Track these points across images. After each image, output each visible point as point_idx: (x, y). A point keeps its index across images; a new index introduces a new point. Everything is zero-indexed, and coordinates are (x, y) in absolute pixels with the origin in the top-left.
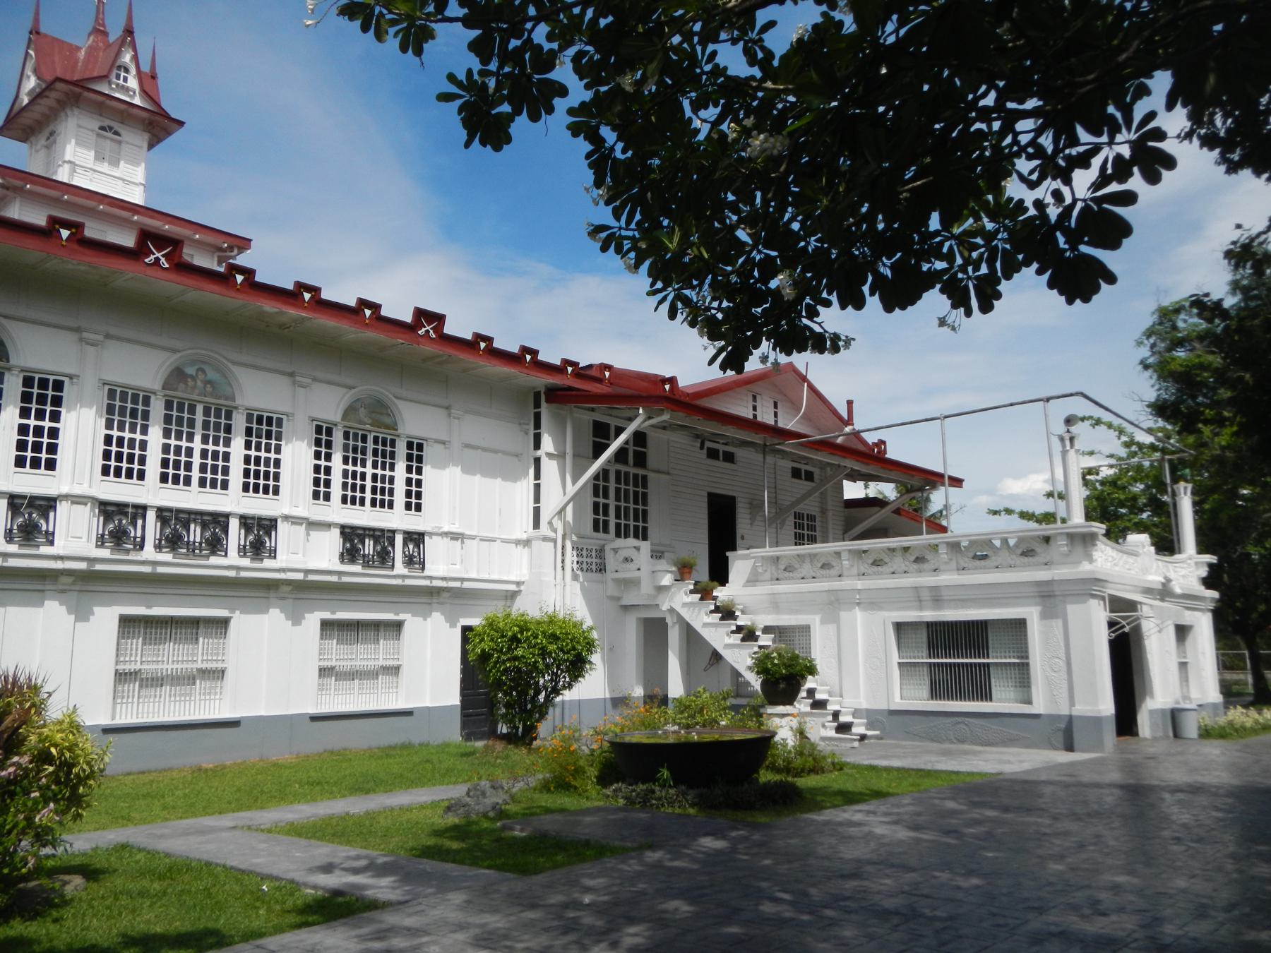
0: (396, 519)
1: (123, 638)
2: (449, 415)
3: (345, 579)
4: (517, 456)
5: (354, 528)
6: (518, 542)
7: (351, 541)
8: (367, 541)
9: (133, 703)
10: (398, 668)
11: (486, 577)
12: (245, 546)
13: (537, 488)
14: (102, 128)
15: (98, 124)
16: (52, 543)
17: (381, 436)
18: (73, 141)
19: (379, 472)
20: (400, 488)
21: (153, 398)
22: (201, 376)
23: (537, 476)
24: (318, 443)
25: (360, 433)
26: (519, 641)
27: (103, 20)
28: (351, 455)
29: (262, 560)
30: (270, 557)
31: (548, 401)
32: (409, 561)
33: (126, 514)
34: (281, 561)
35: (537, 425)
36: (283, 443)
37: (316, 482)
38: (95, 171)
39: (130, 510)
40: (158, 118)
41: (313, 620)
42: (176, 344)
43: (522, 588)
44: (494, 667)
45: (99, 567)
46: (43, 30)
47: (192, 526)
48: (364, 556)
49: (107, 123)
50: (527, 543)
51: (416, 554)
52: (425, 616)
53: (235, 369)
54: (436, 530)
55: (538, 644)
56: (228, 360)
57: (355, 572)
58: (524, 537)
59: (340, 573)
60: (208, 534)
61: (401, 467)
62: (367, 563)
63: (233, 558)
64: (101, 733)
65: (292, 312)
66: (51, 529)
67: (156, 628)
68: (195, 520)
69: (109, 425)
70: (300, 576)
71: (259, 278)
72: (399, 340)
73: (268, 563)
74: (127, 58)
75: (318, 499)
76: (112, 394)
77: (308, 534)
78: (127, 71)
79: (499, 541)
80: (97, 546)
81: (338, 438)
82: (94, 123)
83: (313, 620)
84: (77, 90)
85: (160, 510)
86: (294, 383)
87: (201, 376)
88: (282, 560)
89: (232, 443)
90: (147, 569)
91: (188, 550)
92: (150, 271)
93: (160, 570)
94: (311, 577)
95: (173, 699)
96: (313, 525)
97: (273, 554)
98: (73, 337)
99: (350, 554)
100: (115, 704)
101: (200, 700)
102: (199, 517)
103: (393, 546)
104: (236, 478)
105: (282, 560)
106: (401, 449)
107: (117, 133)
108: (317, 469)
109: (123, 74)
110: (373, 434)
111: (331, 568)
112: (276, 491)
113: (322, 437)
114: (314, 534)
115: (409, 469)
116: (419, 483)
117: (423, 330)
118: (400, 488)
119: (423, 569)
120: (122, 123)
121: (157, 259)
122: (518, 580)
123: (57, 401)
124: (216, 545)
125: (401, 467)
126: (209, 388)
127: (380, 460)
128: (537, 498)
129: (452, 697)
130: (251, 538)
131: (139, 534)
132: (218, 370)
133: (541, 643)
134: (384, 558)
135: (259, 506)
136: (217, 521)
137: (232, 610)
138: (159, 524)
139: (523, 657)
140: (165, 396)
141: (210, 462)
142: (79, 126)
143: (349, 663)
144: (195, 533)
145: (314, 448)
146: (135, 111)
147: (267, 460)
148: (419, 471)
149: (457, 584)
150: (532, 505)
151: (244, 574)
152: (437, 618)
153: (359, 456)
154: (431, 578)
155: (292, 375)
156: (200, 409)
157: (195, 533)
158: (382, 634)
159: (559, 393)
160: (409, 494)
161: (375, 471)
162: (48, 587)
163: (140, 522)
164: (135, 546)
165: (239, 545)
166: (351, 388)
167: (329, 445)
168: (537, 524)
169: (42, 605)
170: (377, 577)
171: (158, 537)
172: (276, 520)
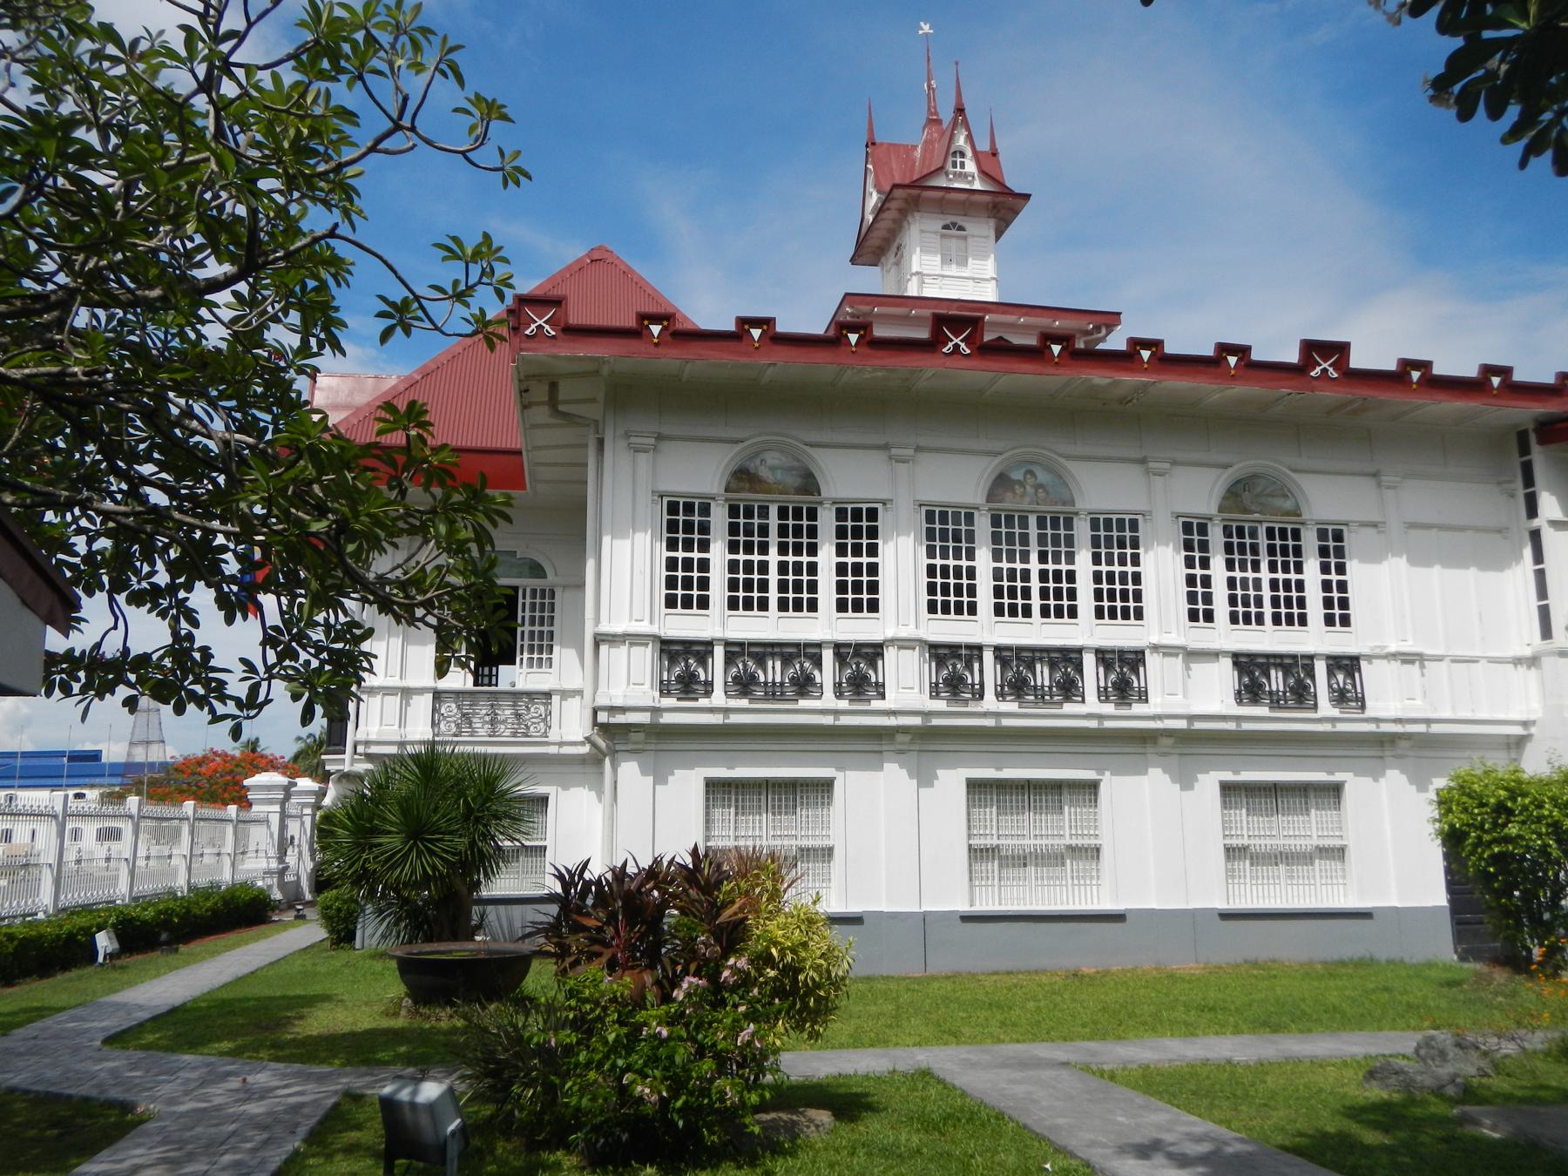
0: (1314, 639)
1: (974, 806)
2: (1379, 485)
3: (1246, 726)
4: (1499, 531)
5: (1252, 656)
6: (1517, 661)
7: (1250, 674)
8: (1273, 672)
9: (993, 885)
10: (1341, 851)
11: (1468, 715)
12: (1106, 688)
13: (1540, 576)
14: (946, 227)
15: (942, 223)
16: (882, 696)
17: (1277, 526)
18: (918, 249)
19: (1280, 576)
21: (976, 514)
22: (1030, 480)
23: (1538, 557)
24: (1188, 546)
25: (1246, 526)
26: (1510, 812)
27: (935, 108)
28: (1236, 557)
29: (1130, 704)
30: (1140, 700)
31: (1542, 441)
32: (1340, 697)
33: (959, 657)
34: (1155, 705)
35: (1529, 480)
36: (1141, 551)
37: (1192, 597)
38: (943, 276)
39: (963, 652)
40: (1000, 199)
41: (1209, 783)
42: (996, 445)
43: (1533, 730)
44: (1472, 853)
45: (936, 722)
46: (878, 140)
47: (1038, 667)
48: (1271, 693)
49: (949, 219)
50: (1533, 661)
51: (1349, 687)
52: (1376, 775)
53: (1073, 466)
54: (1377, 651)
55: (1545, 817)
56: (1060, 455)
58: (1528, 652)
59: (1238, 719)
60: (1058, 676)
62: (1276, 702)
63: (1092, 704)
64: (959, 921)
65: (1129, 379)
66: (881, 680)
67: (1017, 795)
68: (1041, 659)
69: (931, 553)
70: (1181, 724)
72: (1285, 390)
73: (1137, 709)
74: (961, 141)
75: (1237, 623)
76: (930, 517)
77: (1188, 668)
78: (963, 155)
79: (1483, 662)
80: (931, 697)
81: (1216, 537)
82: (935, 223)
83: (1209, 783)
84: (915, 192)
85: (998, 650)
86: (1147, 471)
87: (1030, 480)
88: (1156, 704)
89: (1077, 558)
90: (990, 722)
91: (1036, 696)
92: (950, 362)
93: (1006, 722)
94: (1198, 725)
95: (1076, 882)
96: (1193, 655)
97: (1143, 697)
98: (881, 456)
99: (1251, 691)
100: (972, 887)
101: (1073, 885)
102: (1045, 655)
103: (1313, 678)
105: (1156, 704)
107: (961, 228)
108: (1191, 580)
109: (959, 160)
110: (1265, 525)
111: (1224, 712)
112: (1139, 614)
113: (1193, 538)
114: (1198, 668)
115: (1325, 569)
116: (1342, 586)
117: (1318, 369)
119: (1363, 707)
121: (957, 346)
122: (1524, 717)
123: (873, 532)
124: (1069, 689)
126: (1041, 493)
127: (1279, 559)
128: (1542, 592)
129: (1436, 895)
130: (1113, 677)
131: (977, 681)
132: (1049, 469)
133: (1551, 816)
134: (1301, 695)
136: (1066, 659)
137: (1101, 771)
138: (998, 667)
139: (1520, 837)
140: (990, 509)
141: (1051, 585)
142: (922, 231)
143: (1268, 842)
144: (1043, 675)
145: (1184, 553)
147: (1123, 576)
148: (1341, 569)
149: (1421, 728)
150: (1534, 603)
151: (1108, 724)
152: (1395, 779)
153: (1249, 557)
154: (1377, 720)
155: (1143, 461)
156: (1032, 520)
157: (1043, 675)
158: (1312, 801)
159: (1559, 426)
160: (1328, 603)
161: (1256, 575)
162: (885, 748)
163: (976, 666)
164: (973, 694)
165: (1099, 687)
166: (1226, 466)
167: (1204, 546)
168: (1546, 632)
169: (881, 768)
170: (1293, 721)
171: (999, 682)
172: (1143, 652)
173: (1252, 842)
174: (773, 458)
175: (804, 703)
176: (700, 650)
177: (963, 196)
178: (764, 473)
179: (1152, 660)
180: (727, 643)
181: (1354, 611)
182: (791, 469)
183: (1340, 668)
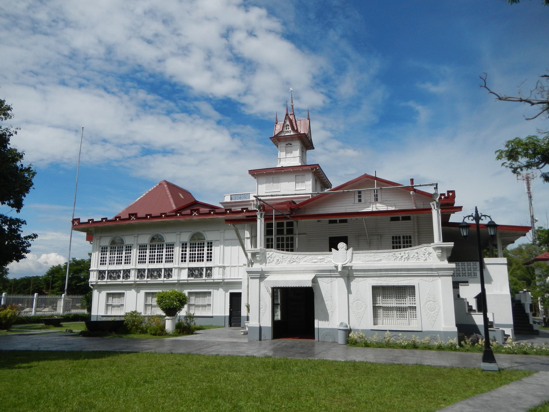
0: (204, 264)
3: (189, 281)
5: (193, 268)
20: (205, 256)
22: (158, 238)
24: (183, 248)
25: (194, 243)
37: (182, 258)
48: (195, 275)
52: (218, 290)
54: (216, 266)
57: (192, 279)
59: (188, 280)
61: (206, 248)
62: (196, 276)
71: (153, 215)
73: (170, 279)
78: (289, 126)
81: (188, 245)
87: (158, 238)
90: (145, 282)
93: (148, 282)
94: (181, 282)
104: (164, 260)
106: (206, 244)
107: (291, 144)
108: (182, 254)
112: (172, 261)
113: (184, 245)
116: (211, 253)
118: (205, 256)
120: (292, 141)
124: (160, 276)
125: (206, 248)
126: (159, 240)
134: (201, 275)
135: (169, 265)
136: (159, 270)
142: (281, 147)
144: (155, 274)
146: (293, 136)
151: (165, 282)
152: (221, 290)
154: (214, 280)
160: (208, 257)
169: (131, 290)
172: (172, 269)
173: (196, 303)
174: (118, 238)
175: (118, 280)
176: (104, 272)
177: (289, 136)
178: (116, 241)
179: (173, 269)
180: (108, 271)
181: (212, 258)
182: (120, 240)
183: (209, 269)
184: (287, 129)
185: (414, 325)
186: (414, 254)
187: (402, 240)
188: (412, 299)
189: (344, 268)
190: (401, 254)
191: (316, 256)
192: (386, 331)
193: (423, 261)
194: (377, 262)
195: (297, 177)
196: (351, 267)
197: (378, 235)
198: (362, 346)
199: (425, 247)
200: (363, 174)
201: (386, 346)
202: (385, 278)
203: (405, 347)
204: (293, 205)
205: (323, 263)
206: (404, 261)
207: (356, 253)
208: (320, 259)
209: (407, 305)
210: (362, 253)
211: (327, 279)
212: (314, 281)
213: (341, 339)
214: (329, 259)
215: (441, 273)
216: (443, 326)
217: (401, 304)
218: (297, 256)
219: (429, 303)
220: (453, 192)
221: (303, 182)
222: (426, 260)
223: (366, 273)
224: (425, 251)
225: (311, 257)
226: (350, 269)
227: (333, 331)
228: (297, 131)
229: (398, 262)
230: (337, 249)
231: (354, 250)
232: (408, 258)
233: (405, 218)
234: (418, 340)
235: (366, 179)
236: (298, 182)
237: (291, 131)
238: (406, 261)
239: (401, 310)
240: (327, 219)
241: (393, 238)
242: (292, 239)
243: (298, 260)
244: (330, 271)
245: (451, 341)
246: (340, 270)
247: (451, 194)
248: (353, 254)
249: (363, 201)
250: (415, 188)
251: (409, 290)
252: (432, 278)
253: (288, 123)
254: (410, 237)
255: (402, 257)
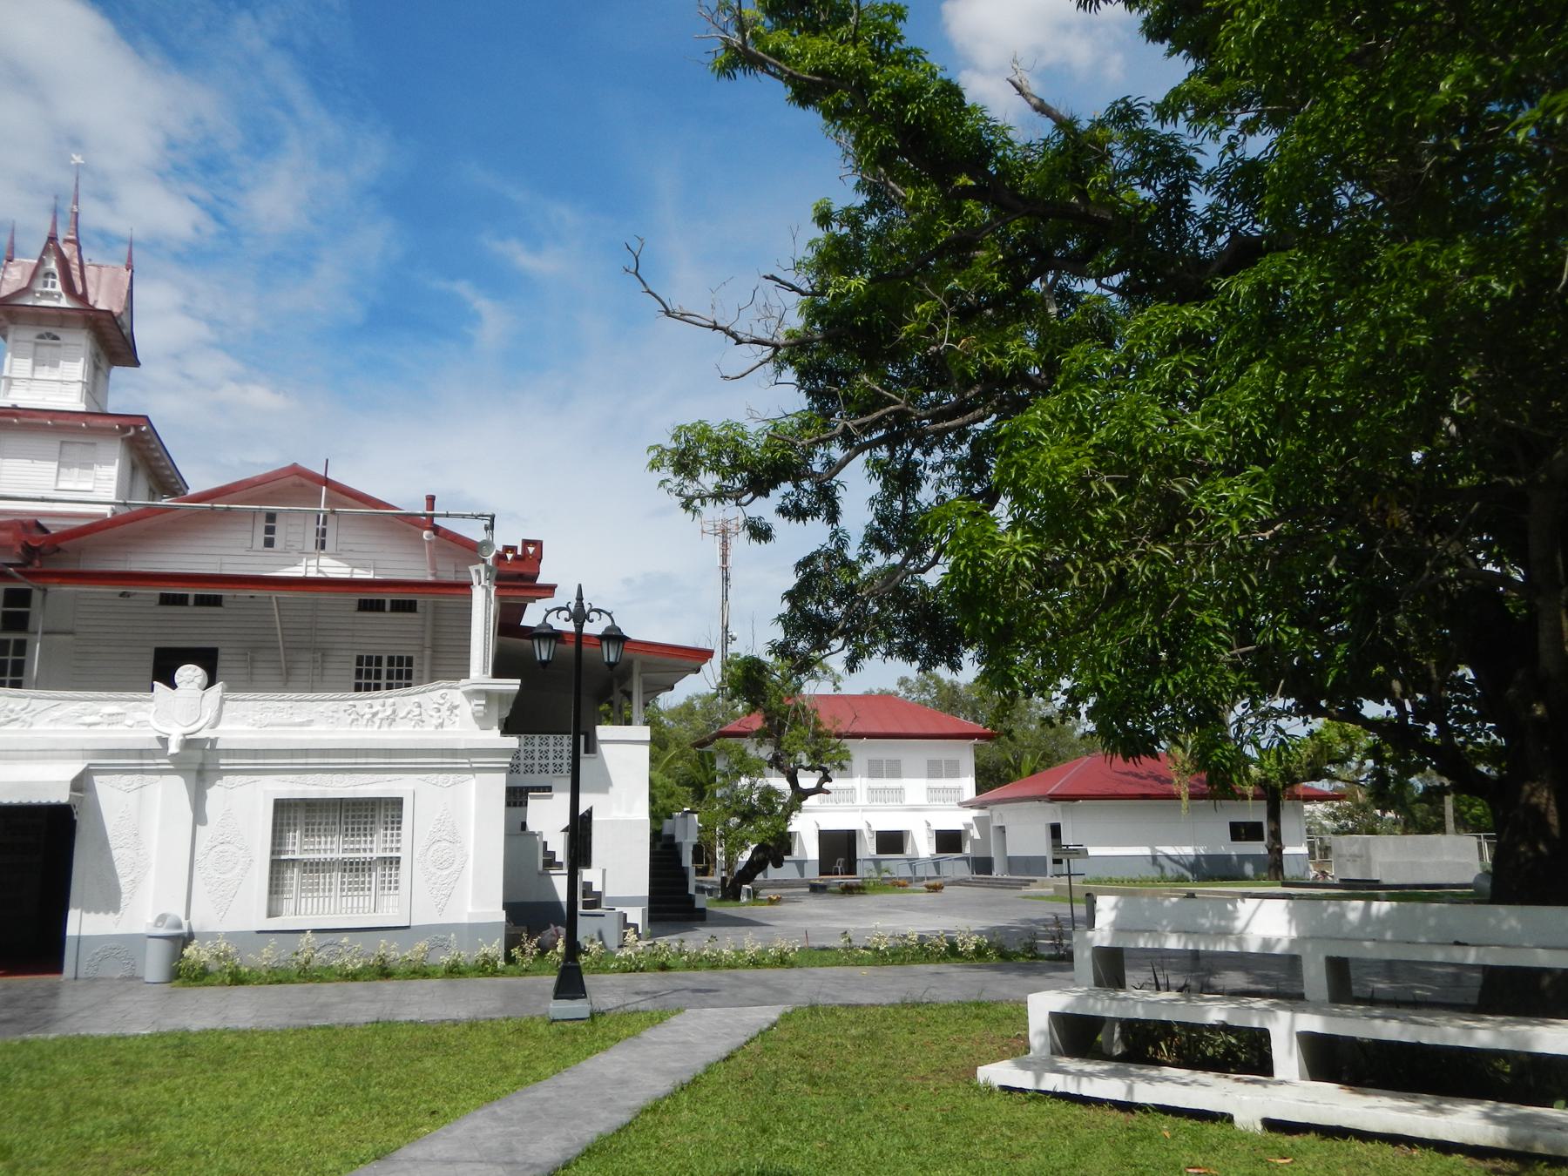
14: (41, 337)
15: (35, 333)
18: (9, 355)
49: (44, 330)
78: (54, 276)
107: (56, 338)
177: (53, 311)
184: (46, 285)
185: (390, 912)
186: (409, 708)
187: (384, 668)
188: (392, 835)
189: (189, 744)
190: (371, 707)
191: (96, 706)
192: (304, 931)
193: (433, 728)
194: (297, 729)
195: (67, 448)
196: (214, 741)
197: (315, 650)
198: (223, 983)
199: (442, 688)
200: (288, 464)
201: (299, 975)
202: (318, 776)
203: (354, 977)
204: (38, 535)
205: (119, 727)
206: (380, 727)
207: (233, 700)
208: (110, 715)
209: (375, 855)
210: (255, 700)
211: (127, 778)
212: (81, 784)
213: (154, 965)
214: (139, 716)
215: (479, 762)
216: (470, 909)
217: (358, 850)
218: (27, 700)
219: (435, 847)
220: (538, 544)
221: (87, 465)
222: (441, 725)
223: (259, 760)
224: (442, 701)
225: (78, 706)
226: (208, 747)
227: (131, 945)
228: (83, 298)
229: (361, 729)
230: (173, 686)
231: (231, 688)
232: (391, 720)
233: (399, 606)
234: (394, 951)
235: (296, 479)
236: (70, 466)
237: (60, 296)
238: (385, 728)
239: (355, 868)
240: (156, 591)
241: (359, 660)
242: (21, 647)
243: (23, 716)
244: (141, 753)
245: (485, 949)
246: (173, 748)
247: (531, 550)
248: (222, 701)
249: (278, 544)
250: (437, 521)
251: (386, 810)
252: (452, 776)
253: (52, 266)
254: (410, 661)
255: (375, 715)
